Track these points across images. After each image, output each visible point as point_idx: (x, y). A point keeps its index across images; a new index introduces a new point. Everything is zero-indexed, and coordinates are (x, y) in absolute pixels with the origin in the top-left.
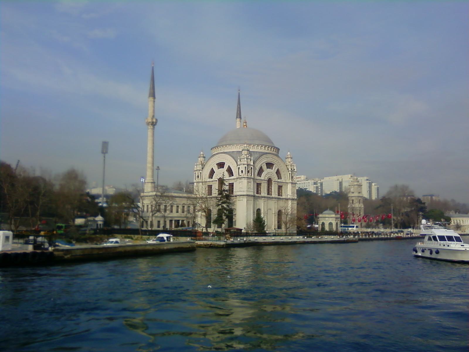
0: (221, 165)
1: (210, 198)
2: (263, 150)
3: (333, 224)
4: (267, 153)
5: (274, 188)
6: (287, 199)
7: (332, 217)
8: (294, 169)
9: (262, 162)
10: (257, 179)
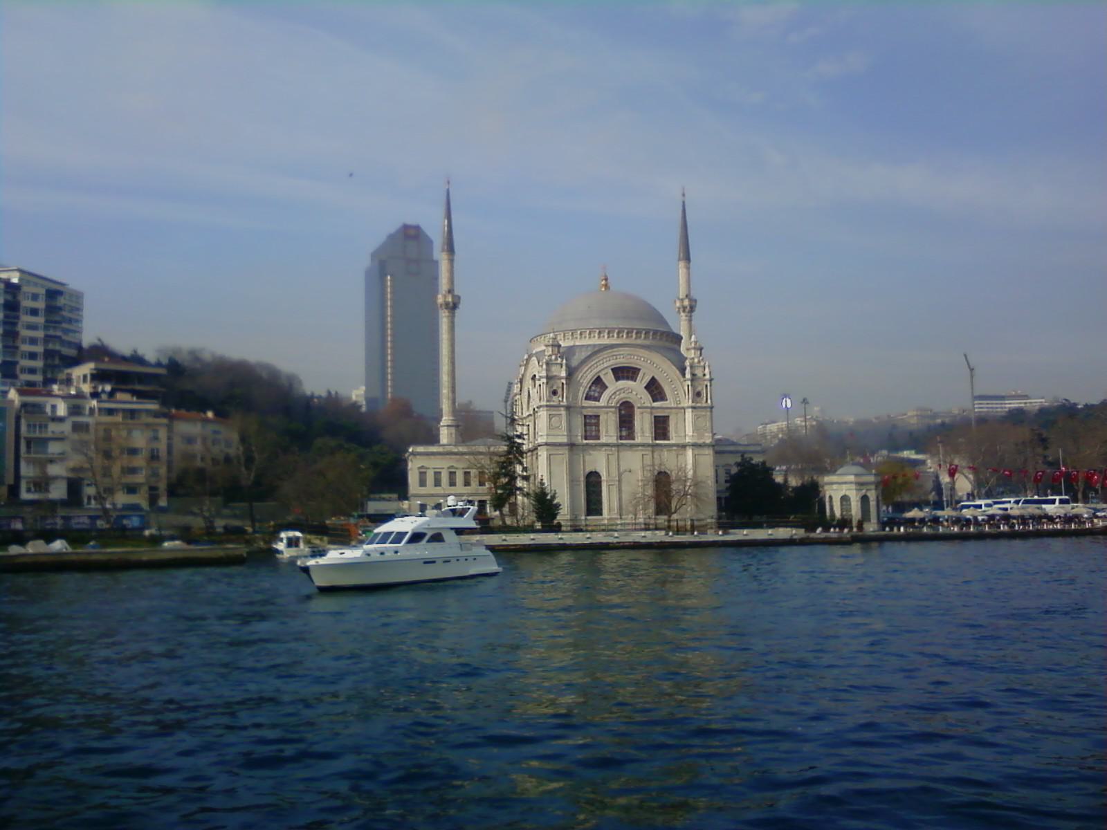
3: (852, 499)
4: (612, 346)
5: (643, 426)
6: (684, 446)
7: (845, 483)
8: (704, 375)
9: (599, 368)
10: (583, 407)
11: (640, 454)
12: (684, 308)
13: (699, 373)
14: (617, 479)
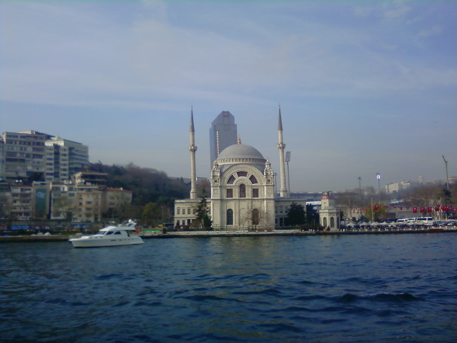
2: (231, 163)
3: (327, 219)
4: (237, 164)
5: (249, 193)
6: (263, 200)
8: (271, 174)
9: (233, 172)
10: (226, 186)
11: (260, 202)
12: (280, 148)
13: (269, 173)
14: (238, 211)
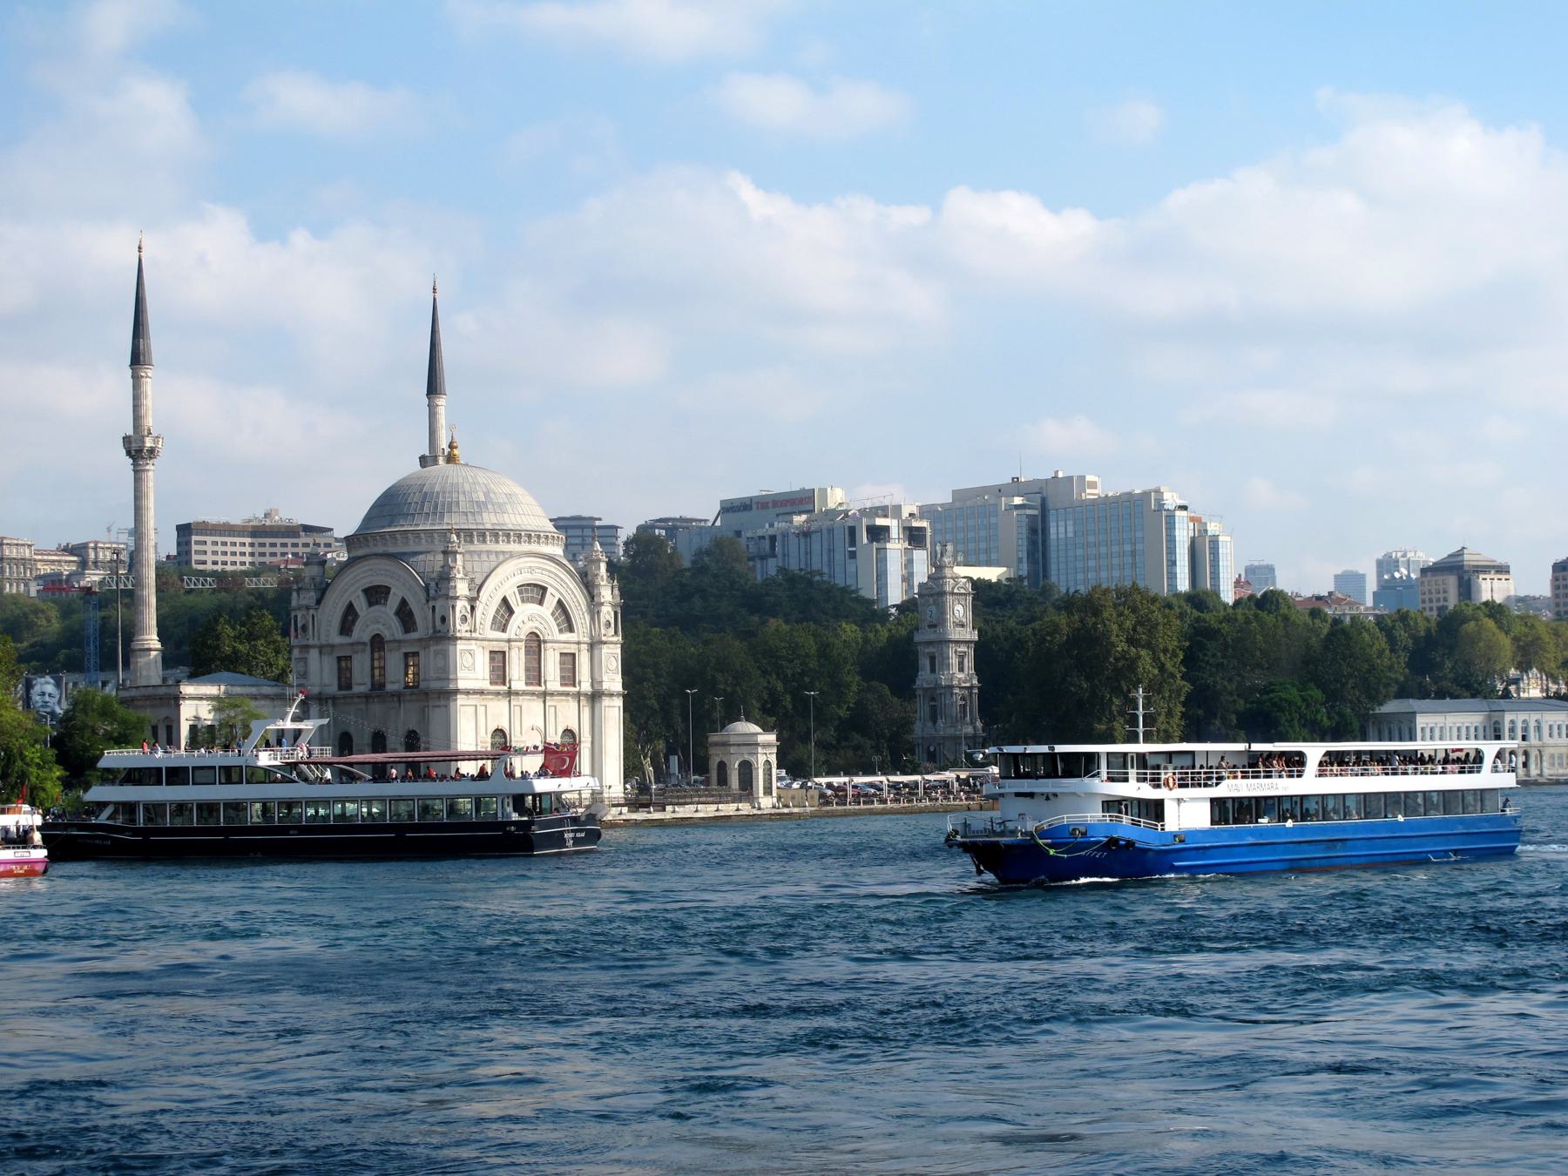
0: (376, 594)
1: (344, 697)
